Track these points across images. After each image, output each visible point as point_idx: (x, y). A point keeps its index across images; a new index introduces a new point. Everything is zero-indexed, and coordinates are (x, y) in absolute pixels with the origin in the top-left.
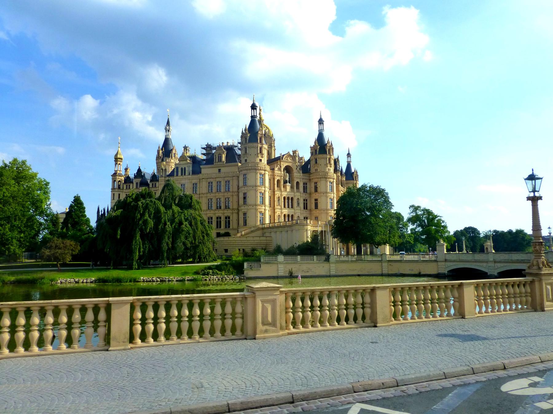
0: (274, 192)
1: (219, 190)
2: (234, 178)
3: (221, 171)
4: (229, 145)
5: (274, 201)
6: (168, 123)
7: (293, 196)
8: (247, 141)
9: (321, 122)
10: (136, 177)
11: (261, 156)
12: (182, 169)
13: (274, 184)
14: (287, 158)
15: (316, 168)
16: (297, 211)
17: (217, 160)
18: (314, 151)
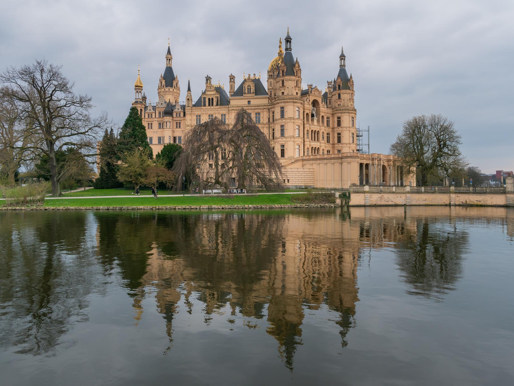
3: (251, 103)
6: (169, 52)
7: (319, 130)
9: (343, 58)
12: (209, 99)
14: (314, 92)
17: (246, 91)
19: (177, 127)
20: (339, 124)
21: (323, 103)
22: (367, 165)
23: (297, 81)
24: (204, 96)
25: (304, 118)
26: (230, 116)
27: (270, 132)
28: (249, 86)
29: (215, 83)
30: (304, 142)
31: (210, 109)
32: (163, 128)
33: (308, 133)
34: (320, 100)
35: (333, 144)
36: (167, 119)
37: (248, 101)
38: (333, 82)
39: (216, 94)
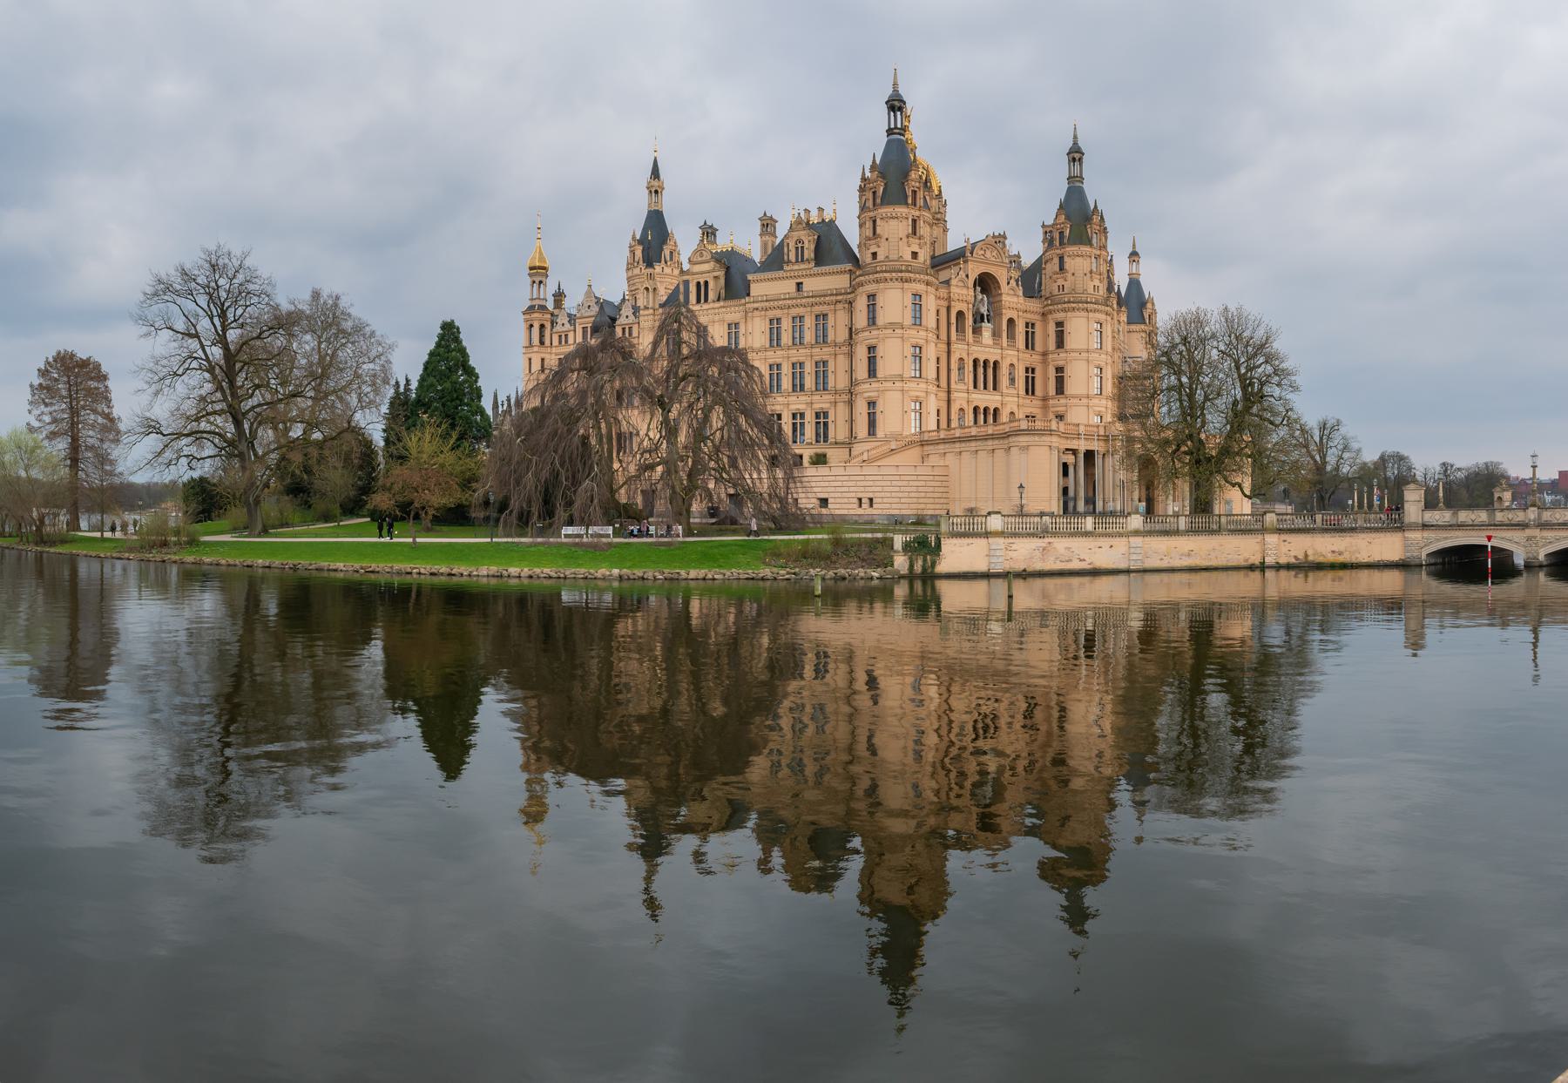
0: (949, 344)
1: (798, 341)
2: (839, 306)
5: (949, 370)
6: (655, 173)
7: (998, 358)
8: (878, 201)
9: (1077, 156)
12: (698, 284)
13: (949, 324)
14: (982, 252)
15: (1060, 282)
16: (1007, 399)
17: (792, 257)
18: (1052, 238)
22: (1089, 455)
28: (799, 241)
39: (714, 271)
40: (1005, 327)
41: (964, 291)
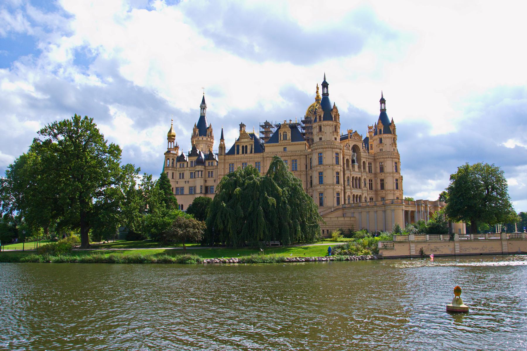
2: (301, 157)
4: (292, 122)
7: (360, 176)
10: (190, 155)
11: (336, 134)
12: (243, 147)
14: (354, 137)
17: (282, 138)
19: (209, 177)
20: (382, 169)
21: (364, 148)
22: (413, 212)
23: (335, 126)
24: (238, 144)
25: (344, 164)
26: (265, 163)
27: (308, 180)
29: (248, 131)
30: (344, 189)
31: (243, 157)
32: (194, 178)
33: (348, 180)
34: (360, 145)
35: (376, 191)
36: (200, 168)
37: (284, 148)
38: (374, 126)
40: (362, 165)
41: (349, 152)
